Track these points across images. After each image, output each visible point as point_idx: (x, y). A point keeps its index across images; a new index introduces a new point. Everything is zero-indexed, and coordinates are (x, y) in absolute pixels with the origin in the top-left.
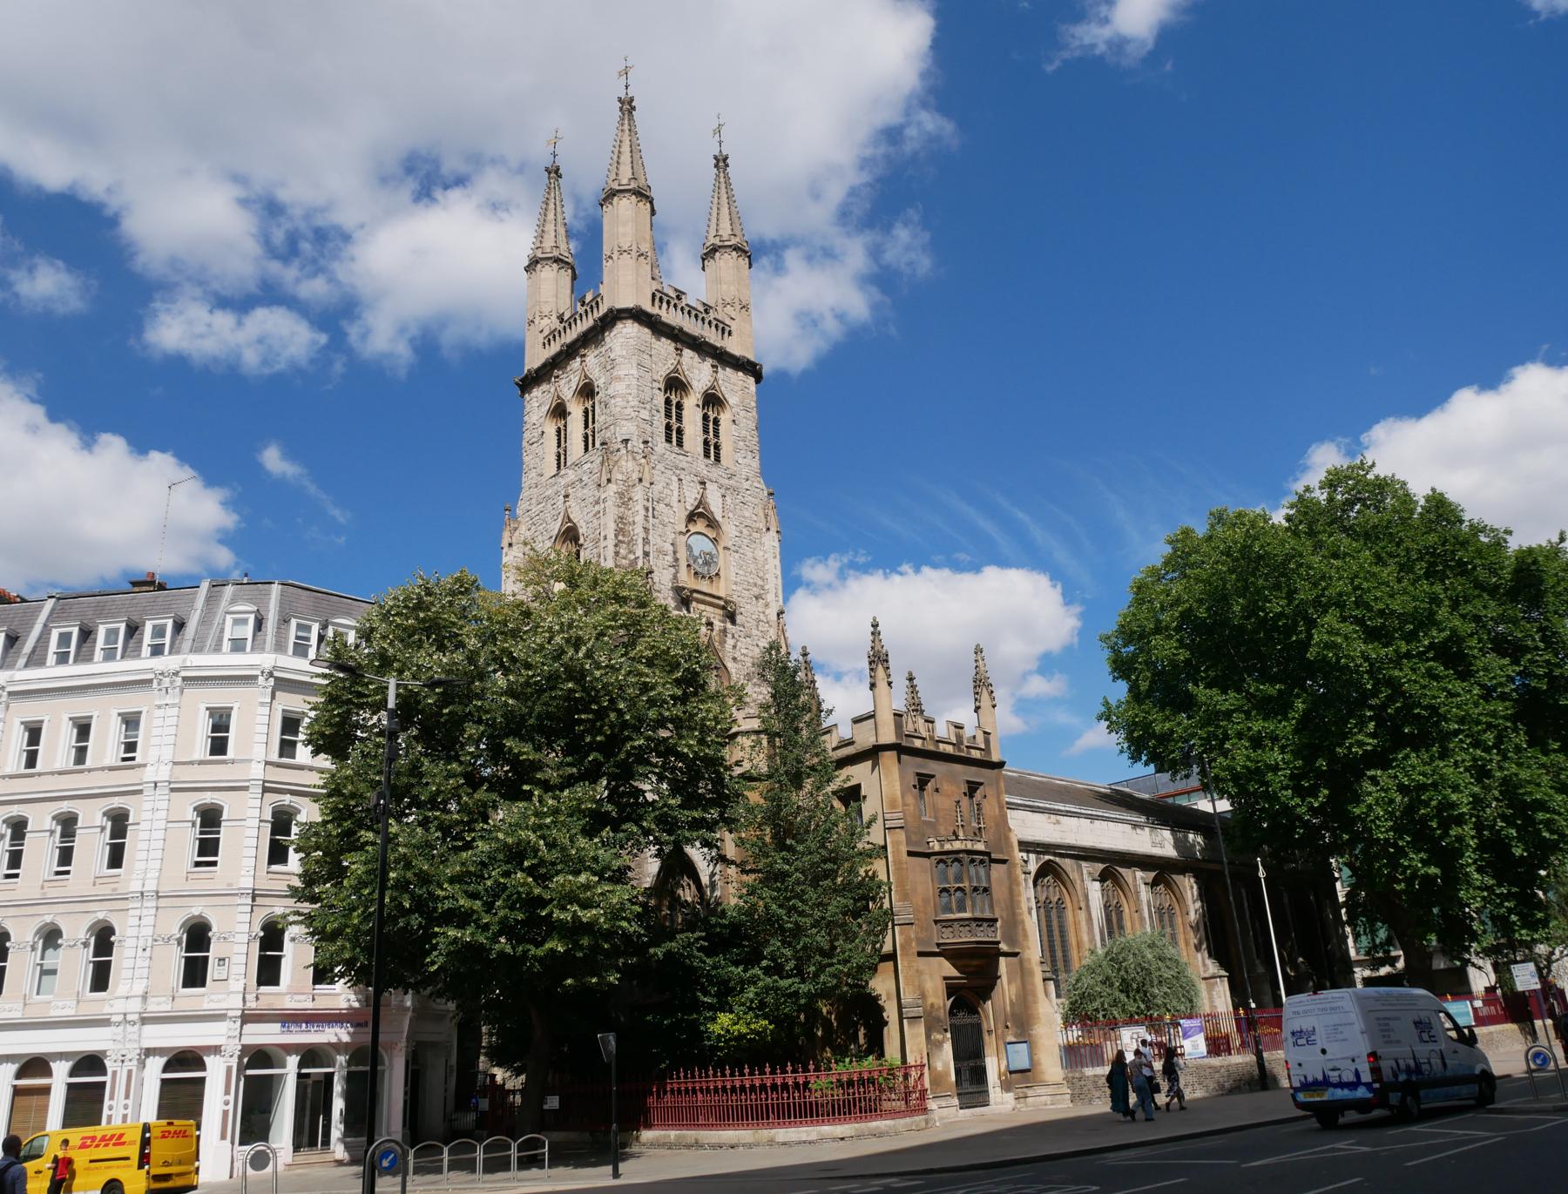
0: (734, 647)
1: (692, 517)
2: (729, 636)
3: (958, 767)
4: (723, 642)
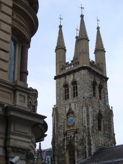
0: (77, 139)
1: (68, 114)
2: (76, 137)
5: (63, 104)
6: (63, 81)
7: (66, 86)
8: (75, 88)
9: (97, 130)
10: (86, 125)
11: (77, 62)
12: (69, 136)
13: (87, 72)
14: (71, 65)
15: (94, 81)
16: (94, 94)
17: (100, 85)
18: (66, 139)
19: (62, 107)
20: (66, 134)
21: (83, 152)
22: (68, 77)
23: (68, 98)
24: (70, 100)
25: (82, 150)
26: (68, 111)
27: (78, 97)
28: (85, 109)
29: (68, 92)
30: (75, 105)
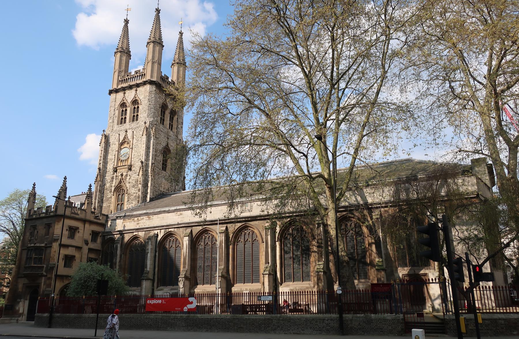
0: (130, 179)
1: (122, 144)
2: (128, 176)
3: (45, 220)
4: (126, 179)
5: (116, 130)
6: (120, 97)
7: (123, 105)
8: (136, 110)
9: (160, 169)
10: (143, 160)
11: (143, 74)
12: (120, 174)
13: (155, 89)
14: (133, 78)
15: (163, 103)
16: (162, 121)
17: (172, 109)
18: (115, 178)
19: (114, 134)
20: (116, 171)
21: (136, 196)
22: (127, 92)
23: (125, 122)
24: (127, 125)
25: (134, 193)
26: (122, 139)
27: (138, 122)
28: (144, 138)
29: (126, 114)
30: (133, 132)
